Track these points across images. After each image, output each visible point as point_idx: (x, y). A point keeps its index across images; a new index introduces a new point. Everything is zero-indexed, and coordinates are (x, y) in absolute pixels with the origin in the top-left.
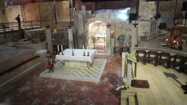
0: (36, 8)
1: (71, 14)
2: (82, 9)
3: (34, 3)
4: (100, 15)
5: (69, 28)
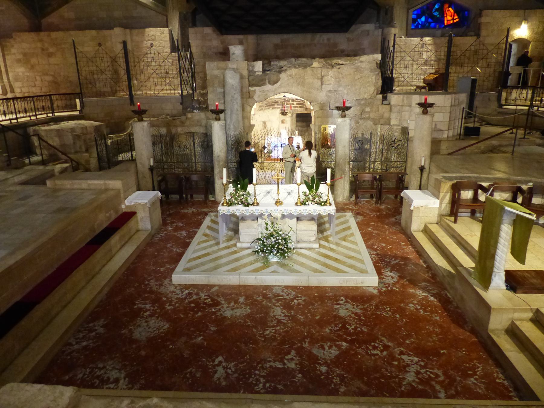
0: (51, 50)
2: (232, 57)
3: (42, 34)
4: (290, 76)
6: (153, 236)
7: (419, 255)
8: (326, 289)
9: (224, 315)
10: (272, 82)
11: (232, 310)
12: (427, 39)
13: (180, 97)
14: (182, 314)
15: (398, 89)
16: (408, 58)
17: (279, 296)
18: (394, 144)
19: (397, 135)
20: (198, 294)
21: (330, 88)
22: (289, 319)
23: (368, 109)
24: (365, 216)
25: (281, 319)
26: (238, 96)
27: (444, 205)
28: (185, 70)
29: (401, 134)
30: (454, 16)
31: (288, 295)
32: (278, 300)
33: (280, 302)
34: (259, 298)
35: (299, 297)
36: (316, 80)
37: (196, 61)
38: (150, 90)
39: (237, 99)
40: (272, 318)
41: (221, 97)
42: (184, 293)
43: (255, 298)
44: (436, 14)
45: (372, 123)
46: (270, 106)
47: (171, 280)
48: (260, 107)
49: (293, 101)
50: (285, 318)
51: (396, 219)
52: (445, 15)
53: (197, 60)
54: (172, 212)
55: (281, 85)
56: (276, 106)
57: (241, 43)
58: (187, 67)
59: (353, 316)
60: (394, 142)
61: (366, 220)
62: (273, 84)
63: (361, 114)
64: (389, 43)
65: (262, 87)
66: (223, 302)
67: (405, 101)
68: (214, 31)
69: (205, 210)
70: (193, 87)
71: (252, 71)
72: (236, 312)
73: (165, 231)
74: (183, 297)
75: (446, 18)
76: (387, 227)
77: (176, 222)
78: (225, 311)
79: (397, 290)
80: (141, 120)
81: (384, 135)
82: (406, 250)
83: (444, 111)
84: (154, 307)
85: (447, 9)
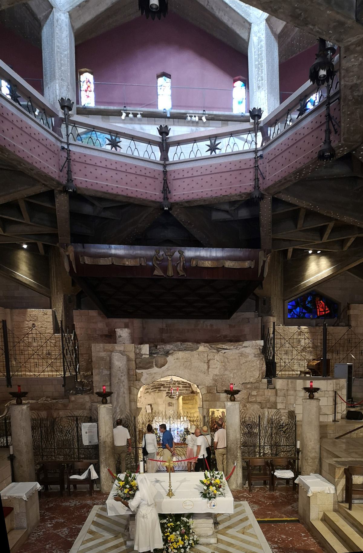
4: (177, 359)
6: (29, 536)
12: (303, 327)
15: (280, 373)
16: (287, 345)
18: (283, 428)
19: (284, 419)
21: (216, 372)
23: (254, 393)
27: (338, 492)
28: (68, 351)
36: (203, 364)
37: (80, 342)
38: (30, 371)
39: (123, 381)
41: (107, 378)
44: (309, 305)
45: (259, 407)
52: (318, 307)
57: (126, 326)
60: (283, 426)
62: (161, 367)
63: (248, 398)
64: (268, 330)
67: (290, 386)
68: (99, 314)
70: (76, 367)
71: (138, 354)
73: (43, 529)
75: (318, 310)
77: (56, 518)
80: (19, 403)
81: (272, 419)
82: (307, 541)
83: (327, 396)
85: (319, 302)
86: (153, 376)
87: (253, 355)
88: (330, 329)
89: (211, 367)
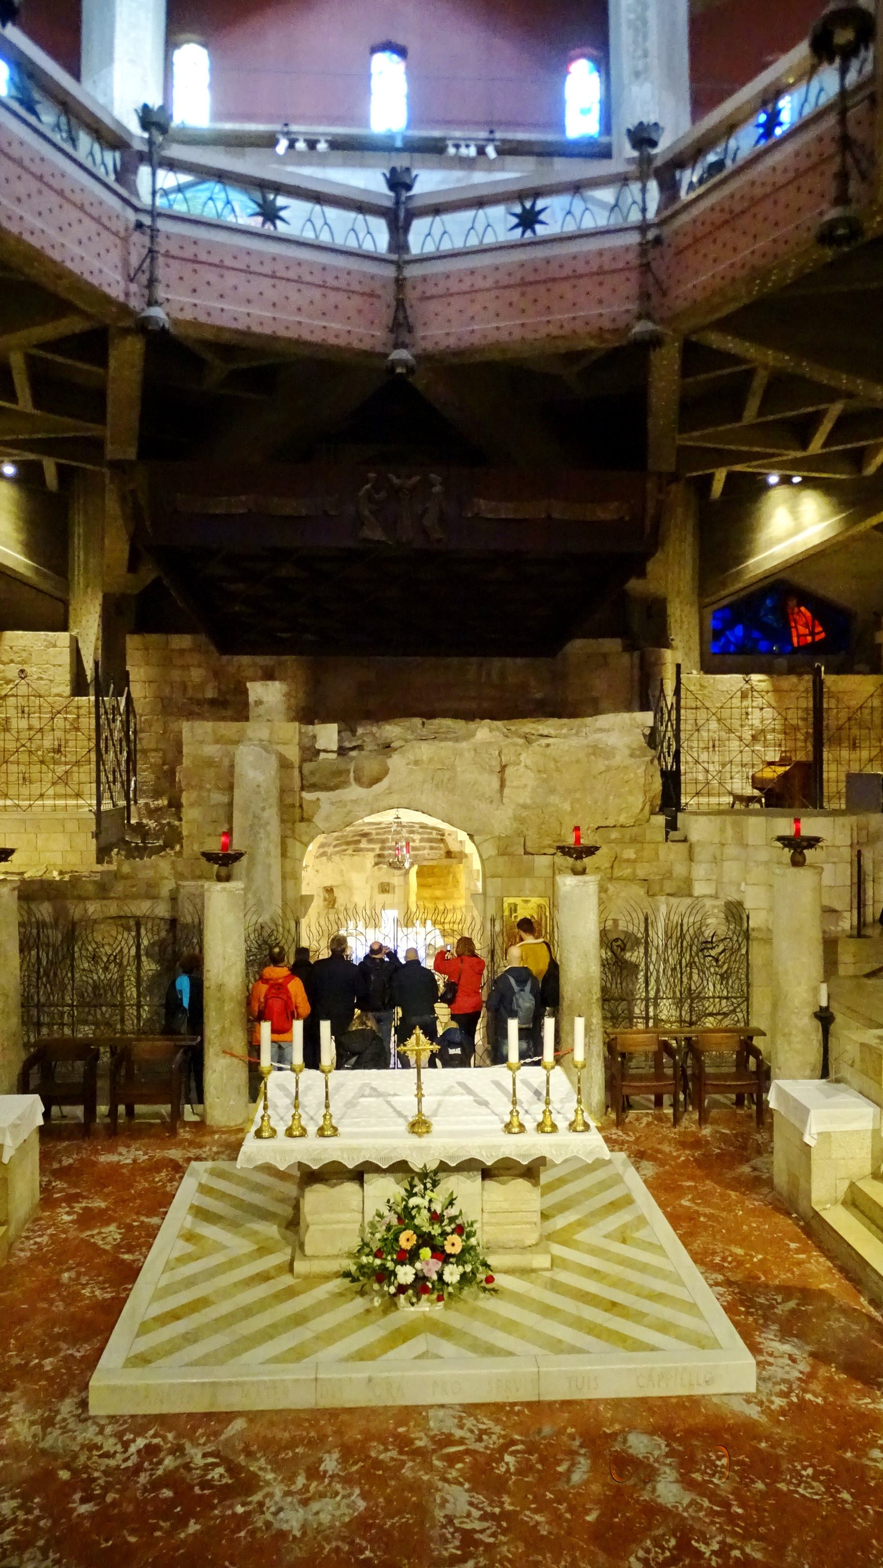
1: (102, 745)
4: (416, 763)
5: (562, 861)
7: (850, 1280)
8: (597, 1411)
9: (276, 1525)
10: (364, 779)
11: (305, 1503)
12: (755, 678)
13: (93, 816)
14: (133, 1532)
15: (693, 802)
16: (714, 725)
17: (453, 1443)
20: (177, 1450)
21: (524, 797)
22: (499, 1526)
24: (662, 1164)
25: (474, 1531)
26: (271, 815)
28: (110, 743)
29: (727, 918)
30: (814, 627)
31: (480, 1439)
32: (451, 1460)
33: (459, 1466)
34: (389, 1454)
35: (513, 1442)
36: (486, 775)
39: (268, 823)
40: (444, 1526)
42: (133, 1449)
43: (373, 1454)
45: (642, 892)
46: (348, 843)
47: (84, 1404)
48: (322, 846)
49: (412, 832)
50: (485, 1524)
51: (755, 1169)
52: (793, 624)
53: (143, 718)
54: (67, 1162)
55: (389, 788)
56: (364, 844)
58: (116, 735)
59: (706, 1503)
60: (712, 942)
61: (666, 1172)
63: (612, 867)
64: (662, 685)
65: (337, 791)
66: (270, 1476)
69: (175, 1154)
72: (317, 1513)
74: (129, 1463)
75: (793, 630)
76: (733, 1195)
78: (280, 1509)
79: (819, 1401)
81: (682, 925)
82: (808, 1265)
83: (835, 860)
84: (29, 1511)
85: (796, 610)
86: (348, 808)
87: (627, 752)
88: (829, 680)
89: (508, 783)
